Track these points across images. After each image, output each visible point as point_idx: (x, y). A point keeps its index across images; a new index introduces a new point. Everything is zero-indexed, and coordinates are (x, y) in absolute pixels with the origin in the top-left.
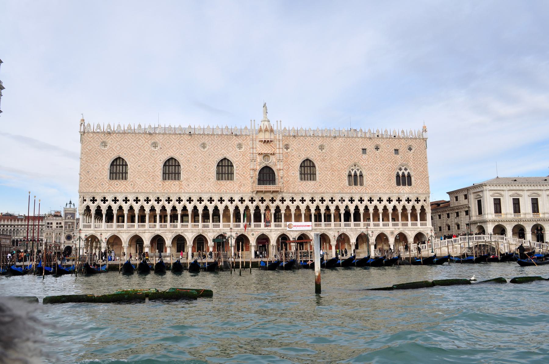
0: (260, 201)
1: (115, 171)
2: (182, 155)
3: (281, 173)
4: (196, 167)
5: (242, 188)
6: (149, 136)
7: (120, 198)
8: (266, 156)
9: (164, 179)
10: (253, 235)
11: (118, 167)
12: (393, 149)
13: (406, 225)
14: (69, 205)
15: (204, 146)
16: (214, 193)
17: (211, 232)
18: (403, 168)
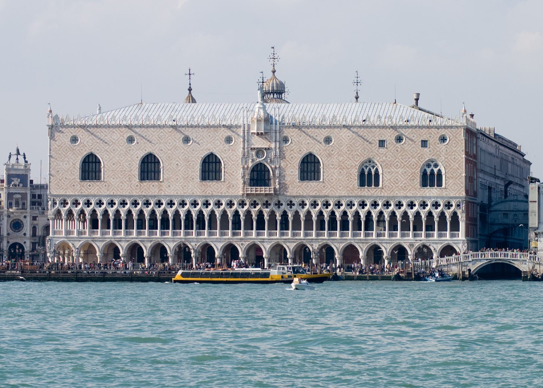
1: (87, 170)
2: (162, 150)
3: (277, 172)
4: (177, 164)
5: (231, 190)
8: (259, 152)
10: (242, 244)
11: (91, 164)
12: (420, 140)
13: (433, 236)
14: (14, 158)
17: (195, 240)
18: (432, 164)
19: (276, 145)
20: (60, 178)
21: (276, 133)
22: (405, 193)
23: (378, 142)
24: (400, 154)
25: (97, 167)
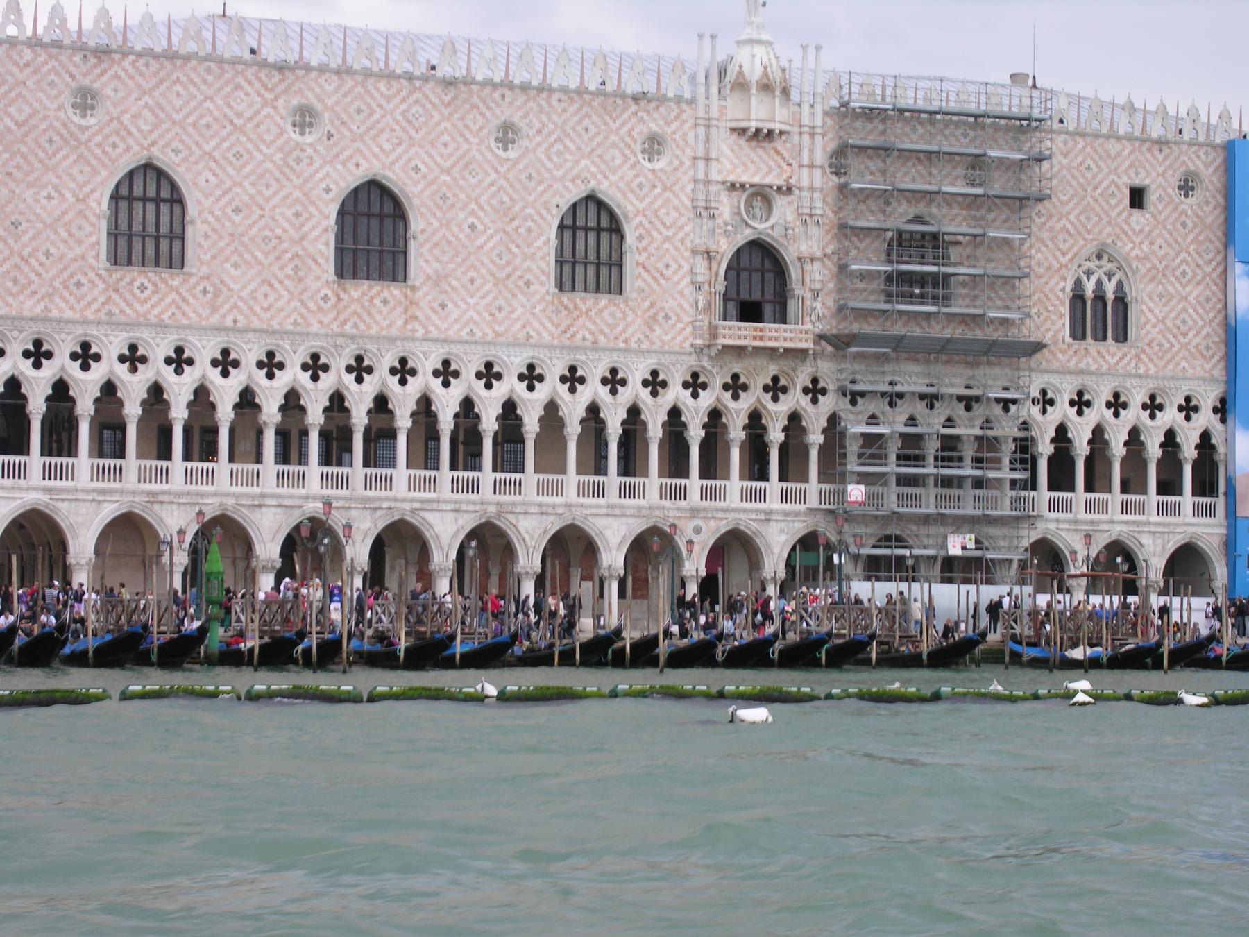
0: (726, 387)
2: (417, 169)
5: (658, 331)
6: (277, 77)
7: (158, 349)
9: (341, 273)
10: (698, 531)
11: (138, 206)
15: (507, 134)
16: (545, 346)
19: (811, 175)
20: (25, 253)
21: (812, 135)
22: (1208, 367)
23: (1127, 192)
24: (1191, 236)
25: (165, 219)
